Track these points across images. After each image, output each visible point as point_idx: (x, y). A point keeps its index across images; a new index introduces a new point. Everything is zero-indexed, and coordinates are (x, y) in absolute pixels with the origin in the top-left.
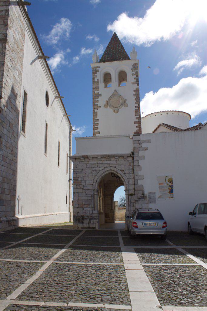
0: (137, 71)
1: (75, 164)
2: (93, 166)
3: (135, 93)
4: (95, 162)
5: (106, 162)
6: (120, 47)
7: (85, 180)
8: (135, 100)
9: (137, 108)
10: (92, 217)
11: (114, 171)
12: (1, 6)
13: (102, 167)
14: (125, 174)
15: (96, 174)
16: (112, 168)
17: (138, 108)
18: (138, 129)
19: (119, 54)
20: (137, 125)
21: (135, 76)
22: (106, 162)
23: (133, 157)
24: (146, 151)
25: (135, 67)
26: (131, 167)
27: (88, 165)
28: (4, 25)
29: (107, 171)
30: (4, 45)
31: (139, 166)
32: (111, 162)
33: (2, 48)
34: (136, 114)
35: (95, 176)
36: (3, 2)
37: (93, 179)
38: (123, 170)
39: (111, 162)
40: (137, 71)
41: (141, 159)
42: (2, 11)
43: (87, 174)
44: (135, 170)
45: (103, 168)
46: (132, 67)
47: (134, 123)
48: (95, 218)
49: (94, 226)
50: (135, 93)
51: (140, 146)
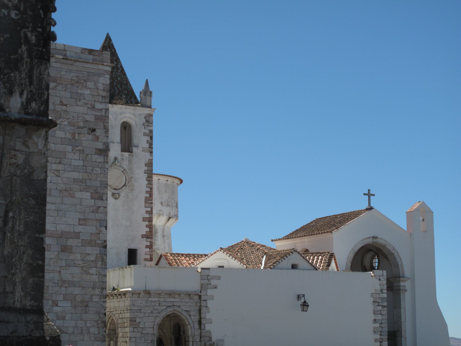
0: (150, 128)
1: (132, 301)
2: (153, 304)
3: (146, 168)
4: (156, 299)
5: (169, 300)
6: (119, 71)
7: (145, 322)
8: (147, 180)
9: (148, 195)
11: (178, 311)
12: (100, 102)
13: (164, 306)
14: (190, 316)
15: (158, 314)
16: (176, 308)
17: (150, 195)
18: (148, 229)
19: (119, 86)
20: (147, 223)
21: (148, 138)
22: (169, 300)
23: (200, 297)
24: (216, 289)
25: (148, 121)
26: (197, 308)
28: (105, 130)
29: (170, 311)
30: (106, 158)
31: (207, 307)
32: (176, 300)
33: (104, 162)
35: (157, 316)
36: (102, 97)
37: (153, 320)
38: (188, 311)
39: (176, 300)
40: (150, 128)
41: (210, 300)
42: (101, 110)
43: (147, 314)
44: (202, 311)
45: (166, 307)
46: (145, 120)
47: (143, 221)
50: (146, 168)
51: (209, 283)
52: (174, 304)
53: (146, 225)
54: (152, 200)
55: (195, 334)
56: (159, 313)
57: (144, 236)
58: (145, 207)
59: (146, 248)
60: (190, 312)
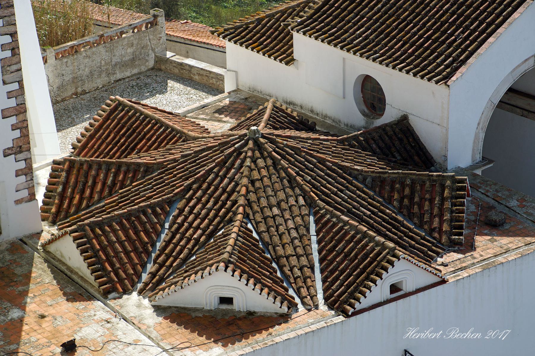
9: (8, 54)
17: (13, 50)
18: (17, 133)
20: (13, 120)
34: (8, 78)
53: (12, 125)
54: (19, 62)
57: (10, 152)
58: (4, 83)
59: (17, 176)
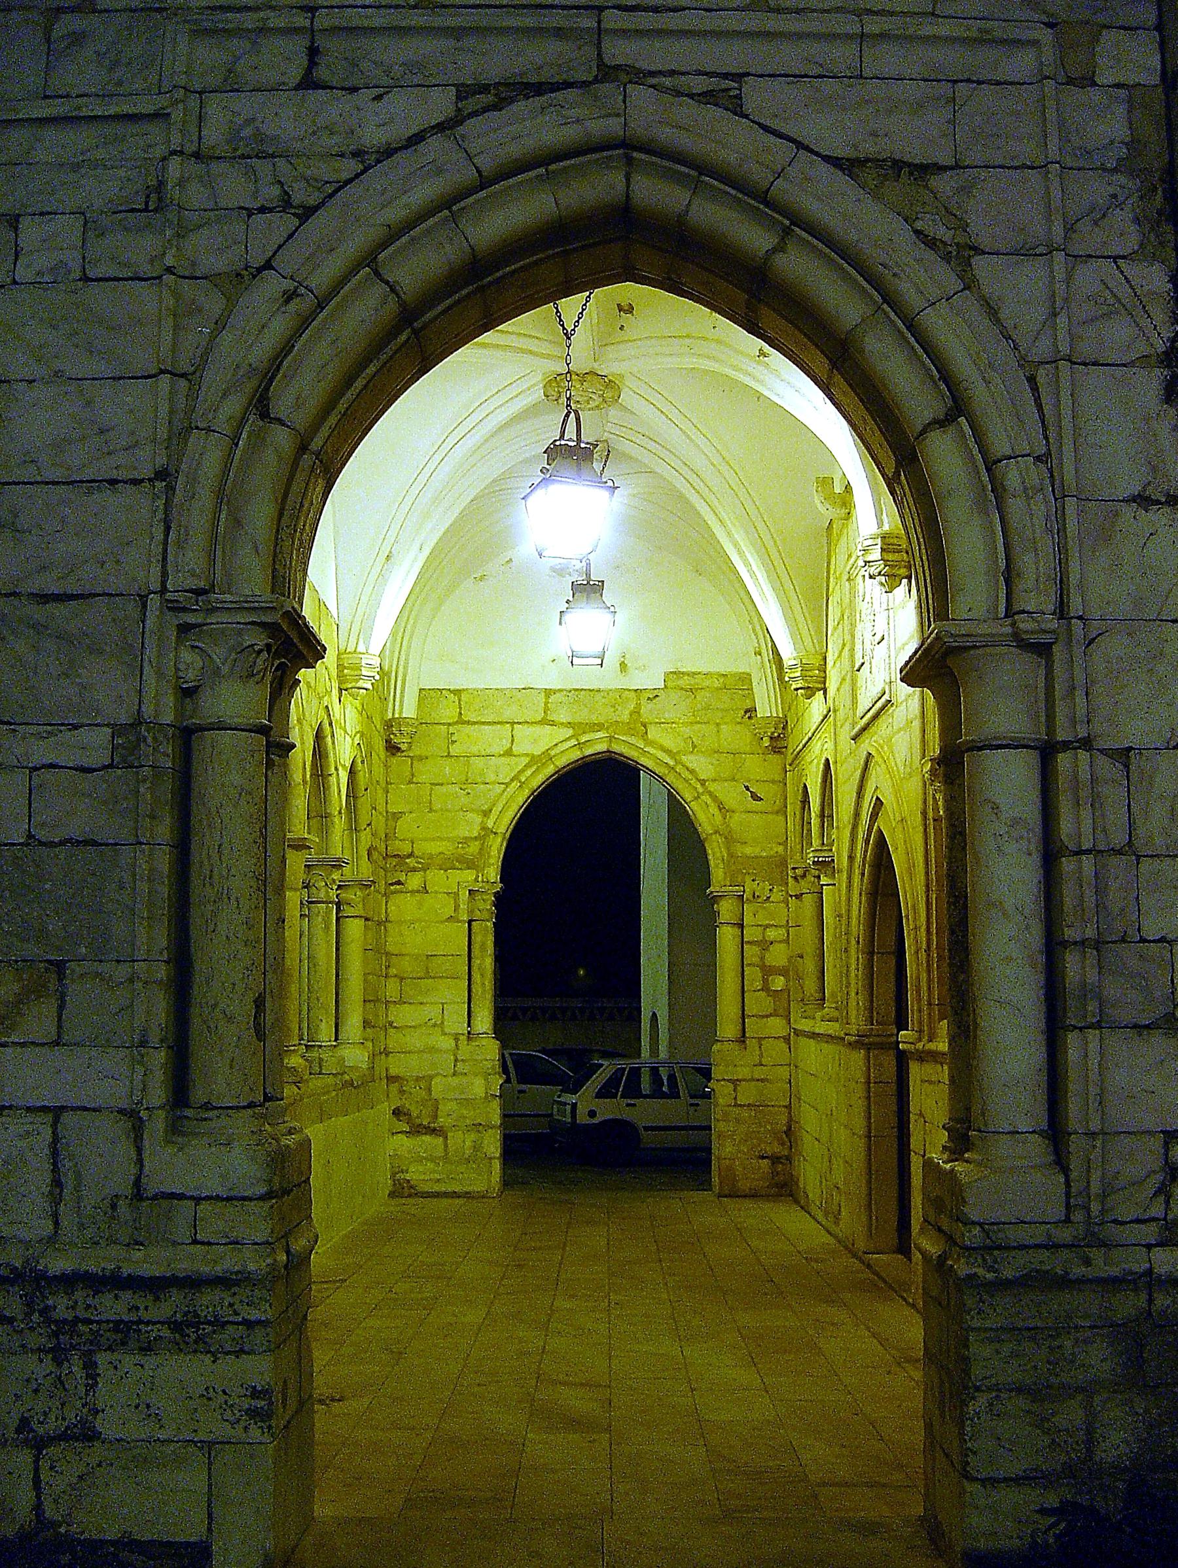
10: (116, 1282)
27: (78, 39)
38: (924, 171)
45: (441, 104)
48: (208, 1301)
49: (191, 1530)
52: (618, 51)
55: (1076, 605)
56: (307, 213)
60: (965, 190)
